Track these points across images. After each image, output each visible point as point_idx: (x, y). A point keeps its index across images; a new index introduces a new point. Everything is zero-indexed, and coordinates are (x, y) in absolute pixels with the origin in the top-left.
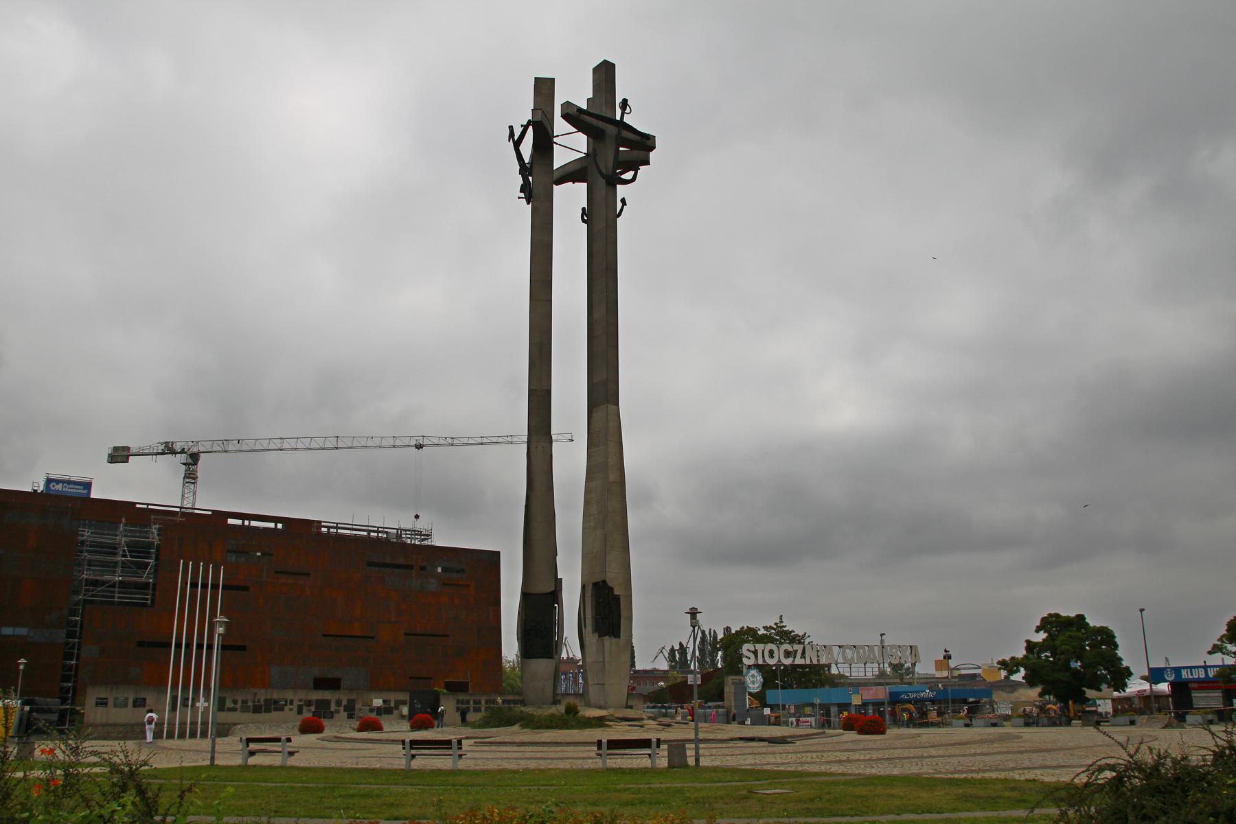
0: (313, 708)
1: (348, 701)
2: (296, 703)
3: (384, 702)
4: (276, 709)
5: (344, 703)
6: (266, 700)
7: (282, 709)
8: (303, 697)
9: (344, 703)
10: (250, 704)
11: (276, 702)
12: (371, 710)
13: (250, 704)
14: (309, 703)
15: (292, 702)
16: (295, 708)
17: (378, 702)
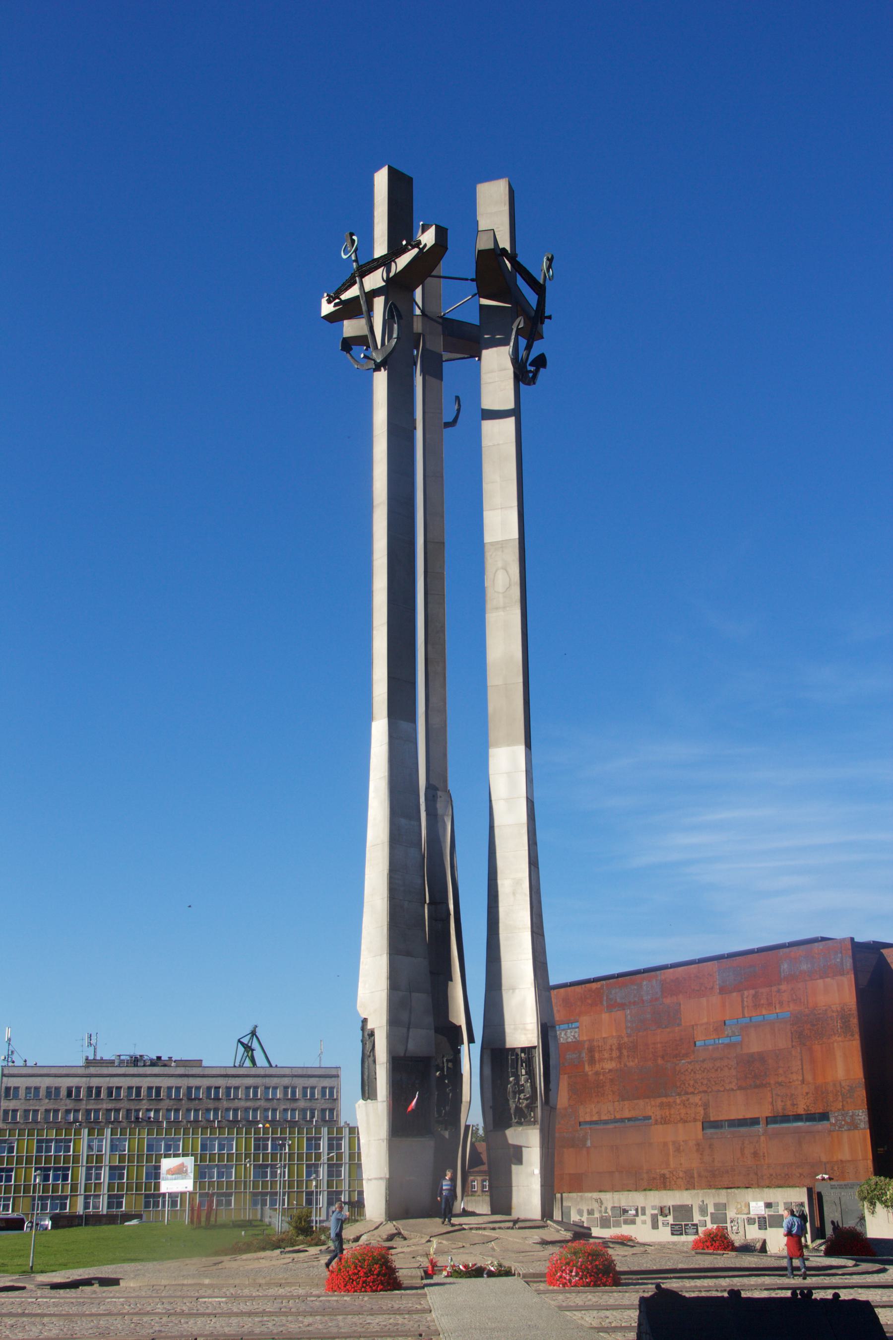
0: (670, 1219)
1: (716, 1205)
2: (649, 1212)
3: (768, 1205)
4: (626, 1222)
5: (711, 1209)
6: (613, 1208)
7: (633, 1222)
8: (658, 1203)
9: (711, 1209)
10: (597, 1215)
11: (625, 1211)
12: (751, 1221)
13: (597, 1215)
14: (662, 1211)
15: (643, 1209)
16: (648, 1218)
17: (757, 1208)
